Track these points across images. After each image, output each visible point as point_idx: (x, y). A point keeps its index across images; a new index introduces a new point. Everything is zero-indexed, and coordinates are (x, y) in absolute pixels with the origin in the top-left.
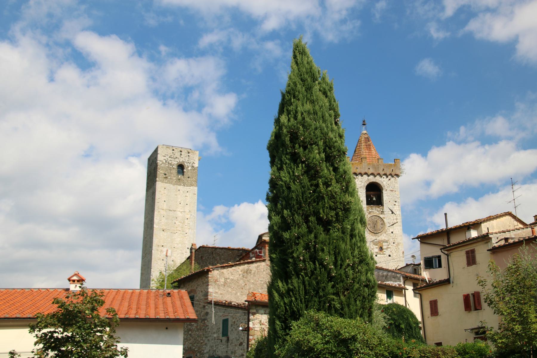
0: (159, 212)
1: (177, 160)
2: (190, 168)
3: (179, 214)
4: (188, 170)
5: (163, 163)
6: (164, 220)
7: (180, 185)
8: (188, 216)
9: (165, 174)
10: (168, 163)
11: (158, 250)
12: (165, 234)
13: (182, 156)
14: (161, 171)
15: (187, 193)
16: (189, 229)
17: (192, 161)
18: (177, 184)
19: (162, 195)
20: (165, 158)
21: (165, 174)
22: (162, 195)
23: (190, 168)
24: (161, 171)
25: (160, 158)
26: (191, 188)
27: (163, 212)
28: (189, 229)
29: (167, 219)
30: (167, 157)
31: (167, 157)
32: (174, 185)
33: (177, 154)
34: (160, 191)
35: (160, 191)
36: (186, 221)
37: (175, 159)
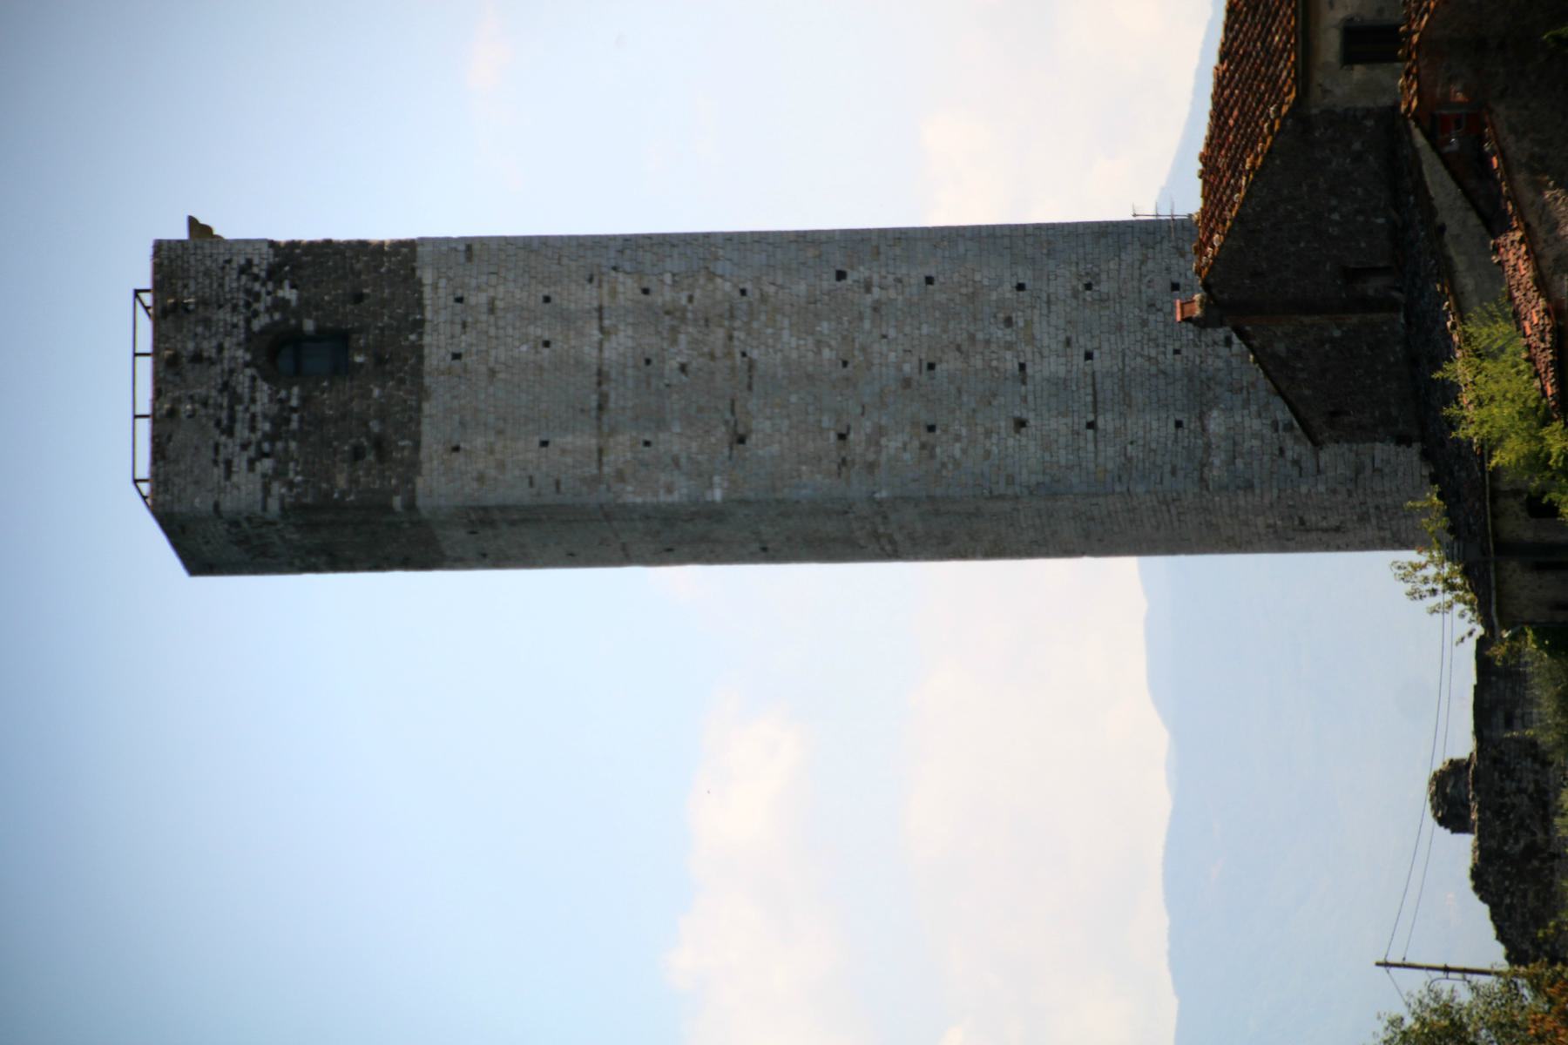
0: (620, 476)
1: (243, 381)
2: (288, 293)
3: (621, 344)
4: (306, 306)
5: (279, 473)
6: (673, 441)
7: (418, 350)
8: (627, 287)
9: (358, 454)
10: (272, 437)
11: (871, 467)
12: (761, 426)
13: (209, 347)
14: (341, 481)
15: (472, 300)
16: (711, 276)
17: (231, 281)
18: (417, 372)
19: (501, 466)
20: (241, 463)
21: (358, 454)
22: (501, 466)
23: (288, 293)
24: (341, 481)
25: (245, 490)
26: (427, 276)
27: (621, 450)
28: (711, 276)
29: (661, 424)
30: (230, 447)
31: (230, 447)
32: (422, 393)
33: (206, 384)
34: (481, 478)
35: (481, 478)
36: (664, 295)
37: (235, 398)
